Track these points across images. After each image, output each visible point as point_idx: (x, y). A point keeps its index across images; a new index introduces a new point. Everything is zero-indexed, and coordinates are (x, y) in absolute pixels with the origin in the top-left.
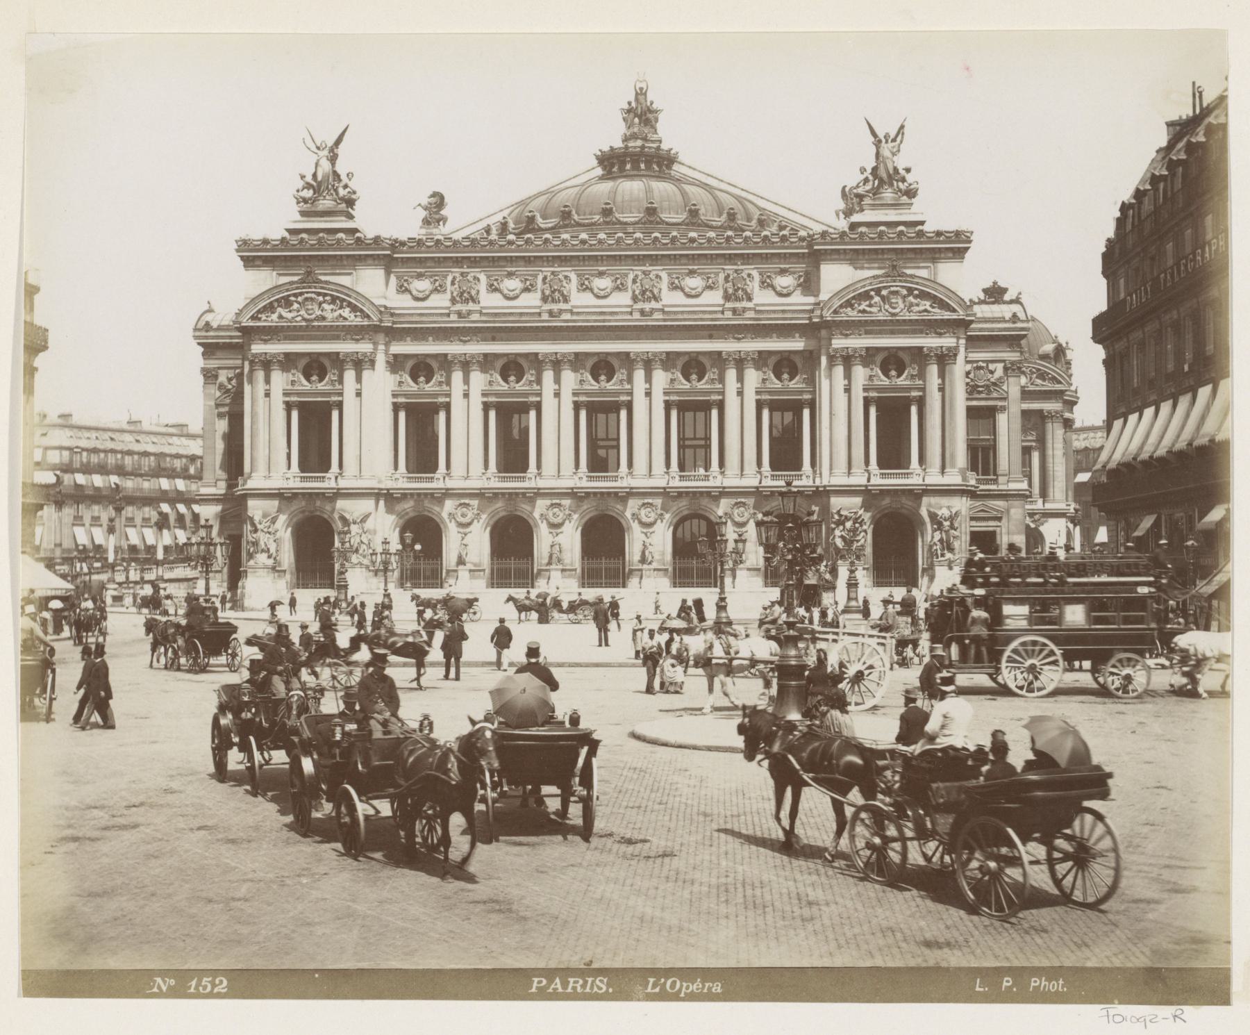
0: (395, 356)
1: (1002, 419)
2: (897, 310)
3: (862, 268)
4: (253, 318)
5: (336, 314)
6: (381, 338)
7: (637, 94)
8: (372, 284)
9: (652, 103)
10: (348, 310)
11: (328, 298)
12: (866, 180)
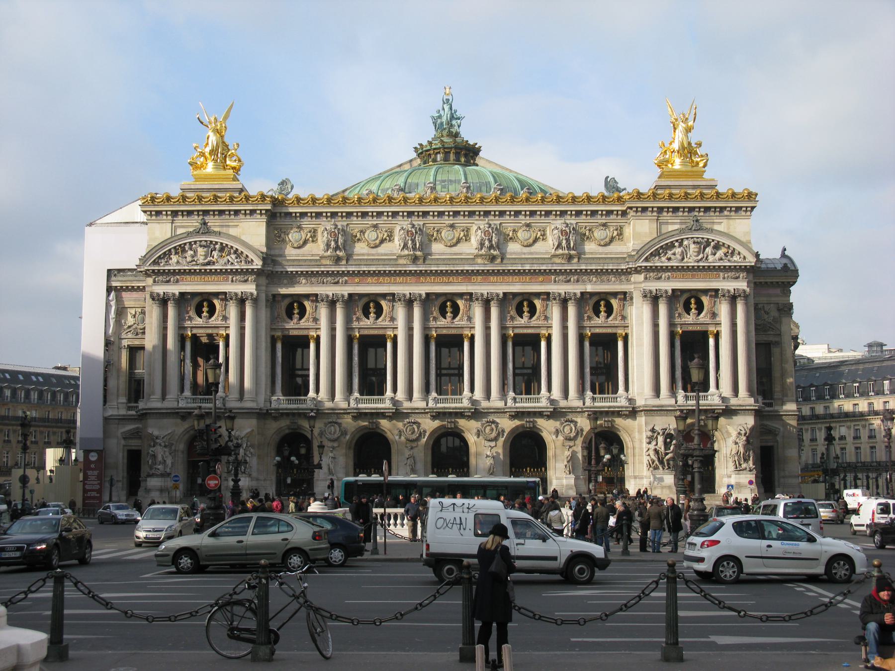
0: (274, 296)
1: (776, 351)
2: (700, 257)
3: (667, 223)
4: (155, 263)
5: (225, 260)
6: (263, 280)
7: (444, 103)
8: (252, 233)
9: (456, 111)
10: (233, 256)
11: (217, 247)
12: (665, 152)
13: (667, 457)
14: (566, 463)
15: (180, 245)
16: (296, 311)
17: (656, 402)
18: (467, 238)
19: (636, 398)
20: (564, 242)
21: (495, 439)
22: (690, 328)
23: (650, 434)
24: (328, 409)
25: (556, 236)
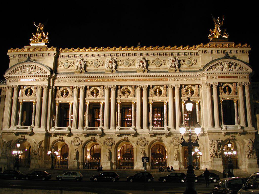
0: (56, 87)
2: (230, 69)
10: (40, 71)
13: (219, 153)
14: (175, 155)
15: (20, 67)
16: (65, 93)
17: (213, 129)
18: (134, 64)
19: (204, 128)
20: (173, 64)
21: (145, 145)
22: (226, 99)
23: (211, 143)
24: (74, 132)
25: (170, 63)
